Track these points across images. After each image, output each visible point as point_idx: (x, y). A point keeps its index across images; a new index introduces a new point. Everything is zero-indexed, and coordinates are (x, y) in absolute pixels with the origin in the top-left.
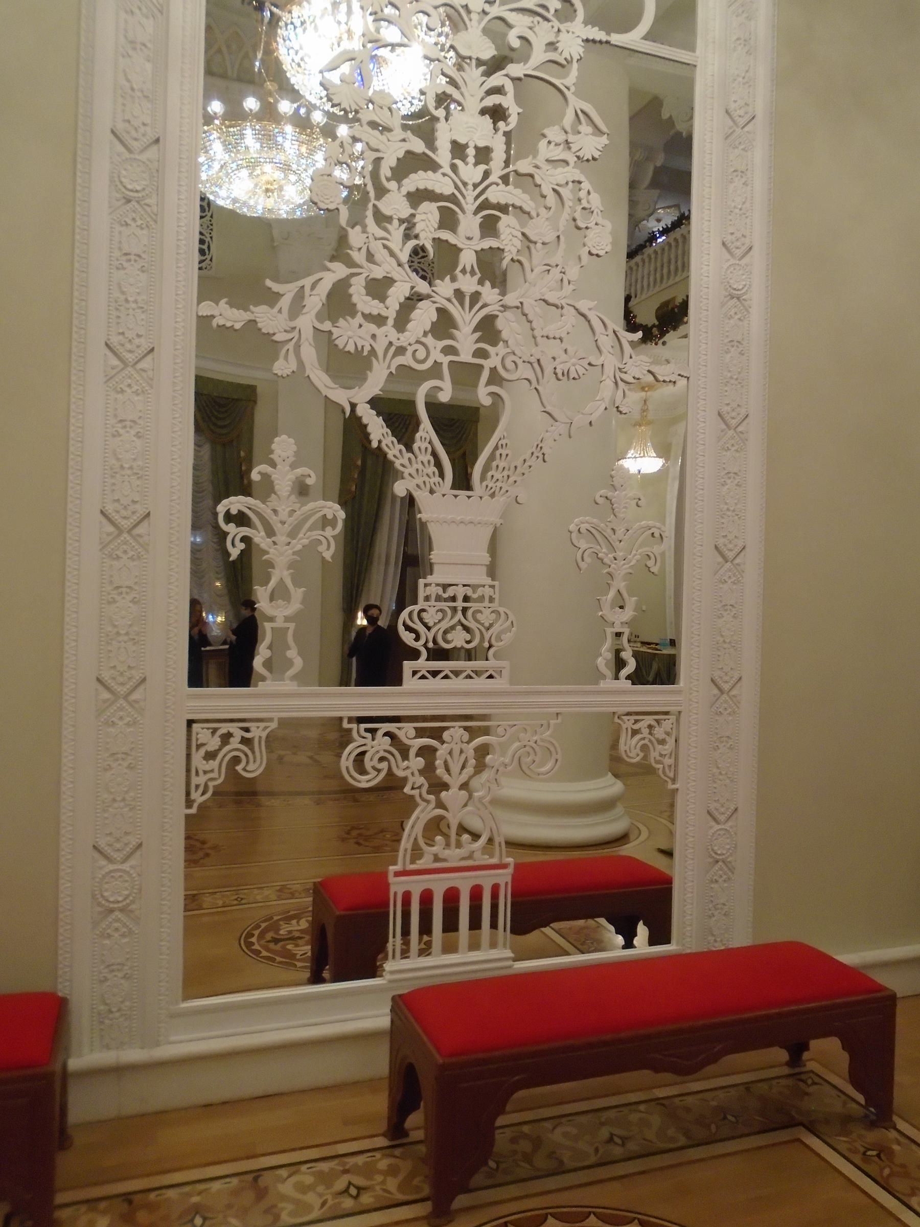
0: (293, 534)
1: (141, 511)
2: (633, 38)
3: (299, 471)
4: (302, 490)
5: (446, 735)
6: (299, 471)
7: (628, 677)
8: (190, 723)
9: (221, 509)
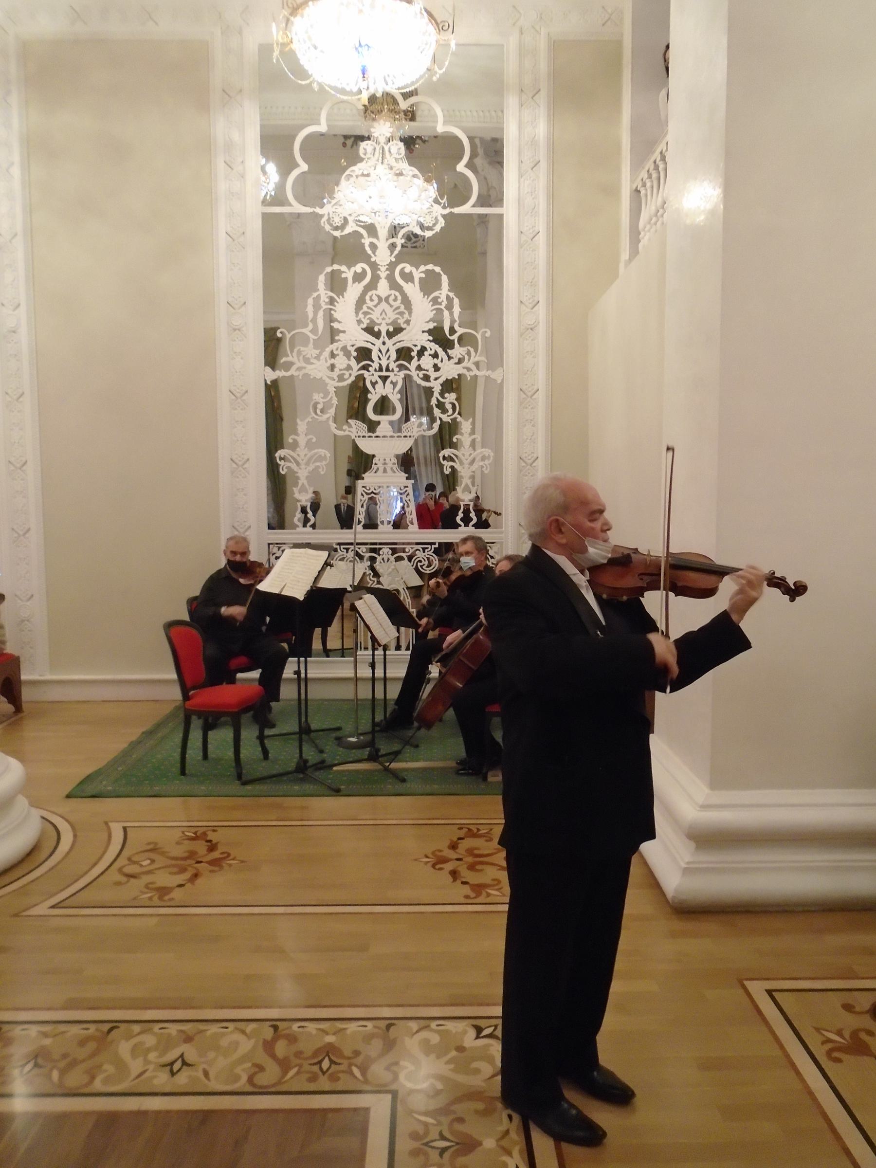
0: (307, 464)
1: (246, 457)
2: (466, 209)
3: (310, 437)
4: (309, 445)
6: (310, 437)
8: (269, 544)
9: (277, 455)
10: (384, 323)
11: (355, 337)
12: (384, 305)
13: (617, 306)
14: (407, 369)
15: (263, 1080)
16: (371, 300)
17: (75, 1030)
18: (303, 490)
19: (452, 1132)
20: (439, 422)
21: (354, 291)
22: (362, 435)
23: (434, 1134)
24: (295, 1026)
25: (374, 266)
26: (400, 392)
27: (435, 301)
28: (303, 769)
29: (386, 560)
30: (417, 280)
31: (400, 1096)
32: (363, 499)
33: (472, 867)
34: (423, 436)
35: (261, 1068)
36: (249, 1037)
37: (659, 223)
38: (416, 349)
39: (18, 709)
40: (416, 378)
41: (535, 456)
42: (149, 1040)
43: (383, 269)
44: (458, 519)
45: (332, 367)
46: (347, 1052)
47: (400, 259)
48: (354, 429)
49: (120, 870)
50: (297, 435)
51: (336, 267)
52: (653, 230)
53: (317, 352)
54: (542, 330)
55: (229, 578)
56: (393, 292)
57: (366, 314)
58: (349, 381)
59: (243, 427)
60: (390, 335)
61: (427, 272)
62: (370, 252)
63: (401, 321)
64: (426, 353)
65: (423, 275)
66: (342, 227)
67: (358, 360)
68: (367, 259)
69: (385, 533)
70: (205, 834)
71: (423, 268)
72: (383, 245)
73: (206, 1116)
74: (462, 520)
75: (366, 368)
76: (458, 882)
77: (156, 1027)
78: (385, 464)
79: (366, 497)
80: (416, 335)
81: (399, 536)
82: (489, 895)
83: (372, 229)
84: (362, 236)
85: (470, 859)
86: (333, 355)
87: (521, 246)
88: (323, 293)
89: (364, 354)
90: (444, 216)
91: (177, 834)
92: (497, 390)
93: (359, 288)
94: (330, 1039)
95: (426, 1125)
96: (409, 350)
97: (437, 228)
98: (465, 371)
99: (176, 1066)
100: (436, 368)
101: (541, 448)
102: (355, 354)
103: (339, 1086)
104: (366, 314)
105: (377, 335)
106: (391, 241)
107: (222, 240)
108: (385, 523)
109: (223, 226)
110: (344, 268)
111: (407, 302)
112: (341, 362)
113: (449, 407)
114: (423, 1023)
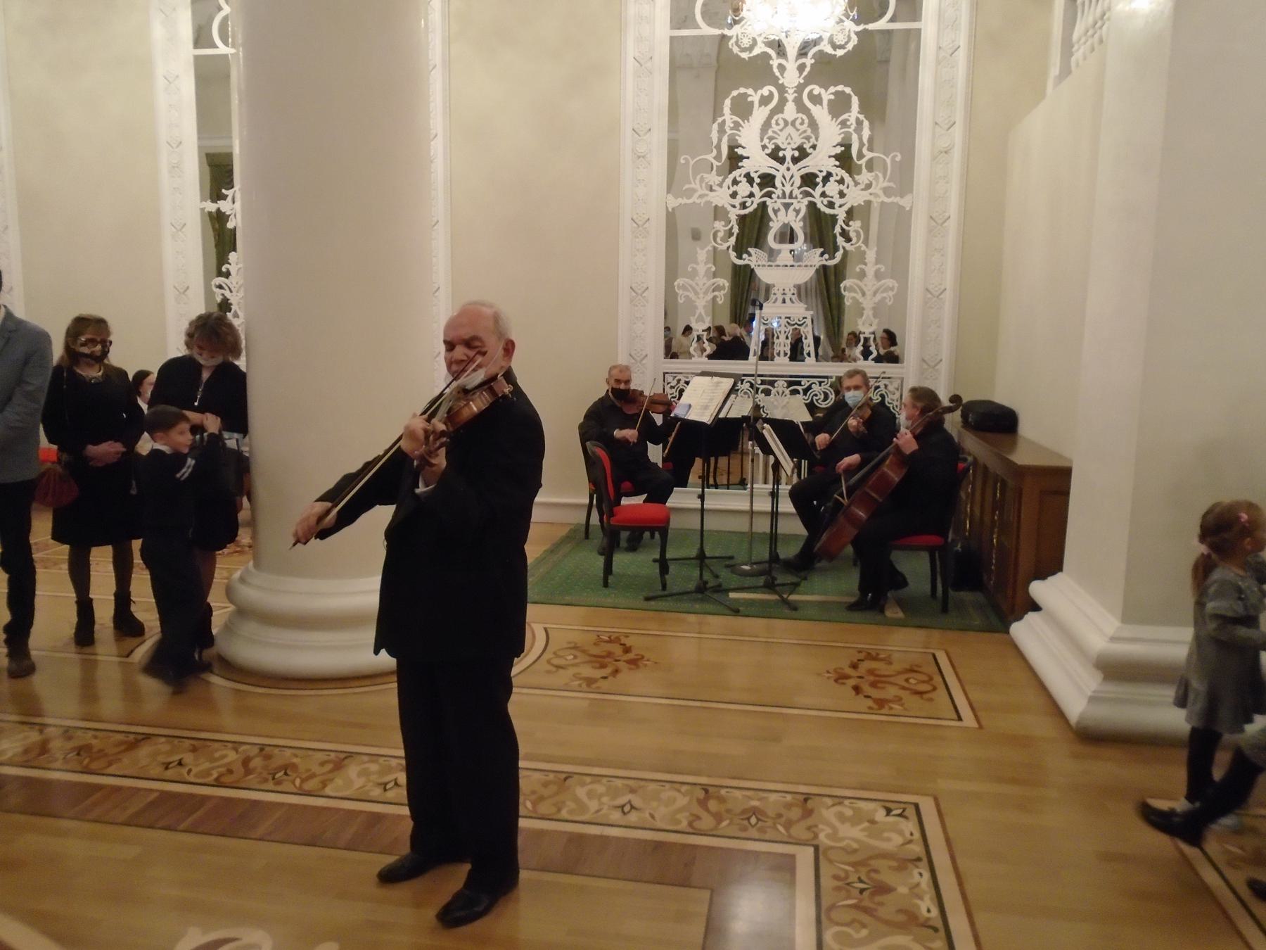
0: (706, 293)
2: (882, 24)
10: (789, 148)
11: (758, 162)
12: (790, 129)
13: (1045, 129)
14: (811, 195)
15: (698, 825)
16: (777, 124)
17: (537, 775)
18: (700, 319)
19: (870, 878)
20: (841, 251)
21: (760, 114)
23: (853, 878)
24: (723, 792)
25: (782, 89)
26: (804, 219)
27: (844, 124)
28: (702, 589)
30: (825, 102)
31: (821, 849)
33: (873, 685)
34: (824, 267)
35: (698, 818)
36: (684, 795)
37: (1097, 36)
38: (821, 175)
40: (820, 206)
42: (600, 789)
43: (791, 91)
45: (734, 195)
46: (771, 813)
47: (809, 80)
48: (754, 258)
49: (549, 662)
50: (697, 263)
51: (742, 90)
52: (1089, 43)
53: (720, 178)
54: (957, 154)
55: (613, 406)
56: (800, 115)
57: (771, 139)
58: (750, 209)
60: (795, 160)
61: (836, 94)
62: (778, 74)
63: (807, 146)
64: (832, 179)
65: (832, 97)
66: (751, 49)
67: (761, 186)
68: (774, 81)
70: (618, 639)
71: (832, 89)
72: (791, 65)
73: (658, 845)
75: (769, 195)
76: (861, 696)
77: (605, 780)
80: (821, 161)
82: (891, 708)
83: (779, 47)
84: (770, 57)
85: (872, 678)
86: (735, 182)
87: (938, 62)
88: (728, 117)
89: (767, 180)
90: (857, 33)
91: (593, 637)
92: (903, 218)
93: (766, 111)
94: (755, 803)
95: (846, 872)
96: (815, 176)
97: (850, 47)
98: (871, 198)
99: (627, 808)
100: (842, 195)
101: (949, 281)
102: (757, 180)
103: (767, 837)
104: (771, 139)
105: (782, 161)
106: (800, 61)
107: (630, 65)
109: (631, 50)
110: (750, 91)
111: (813, 125)
112: (744, 189)
113: (852, 235)
114: (837, 800)
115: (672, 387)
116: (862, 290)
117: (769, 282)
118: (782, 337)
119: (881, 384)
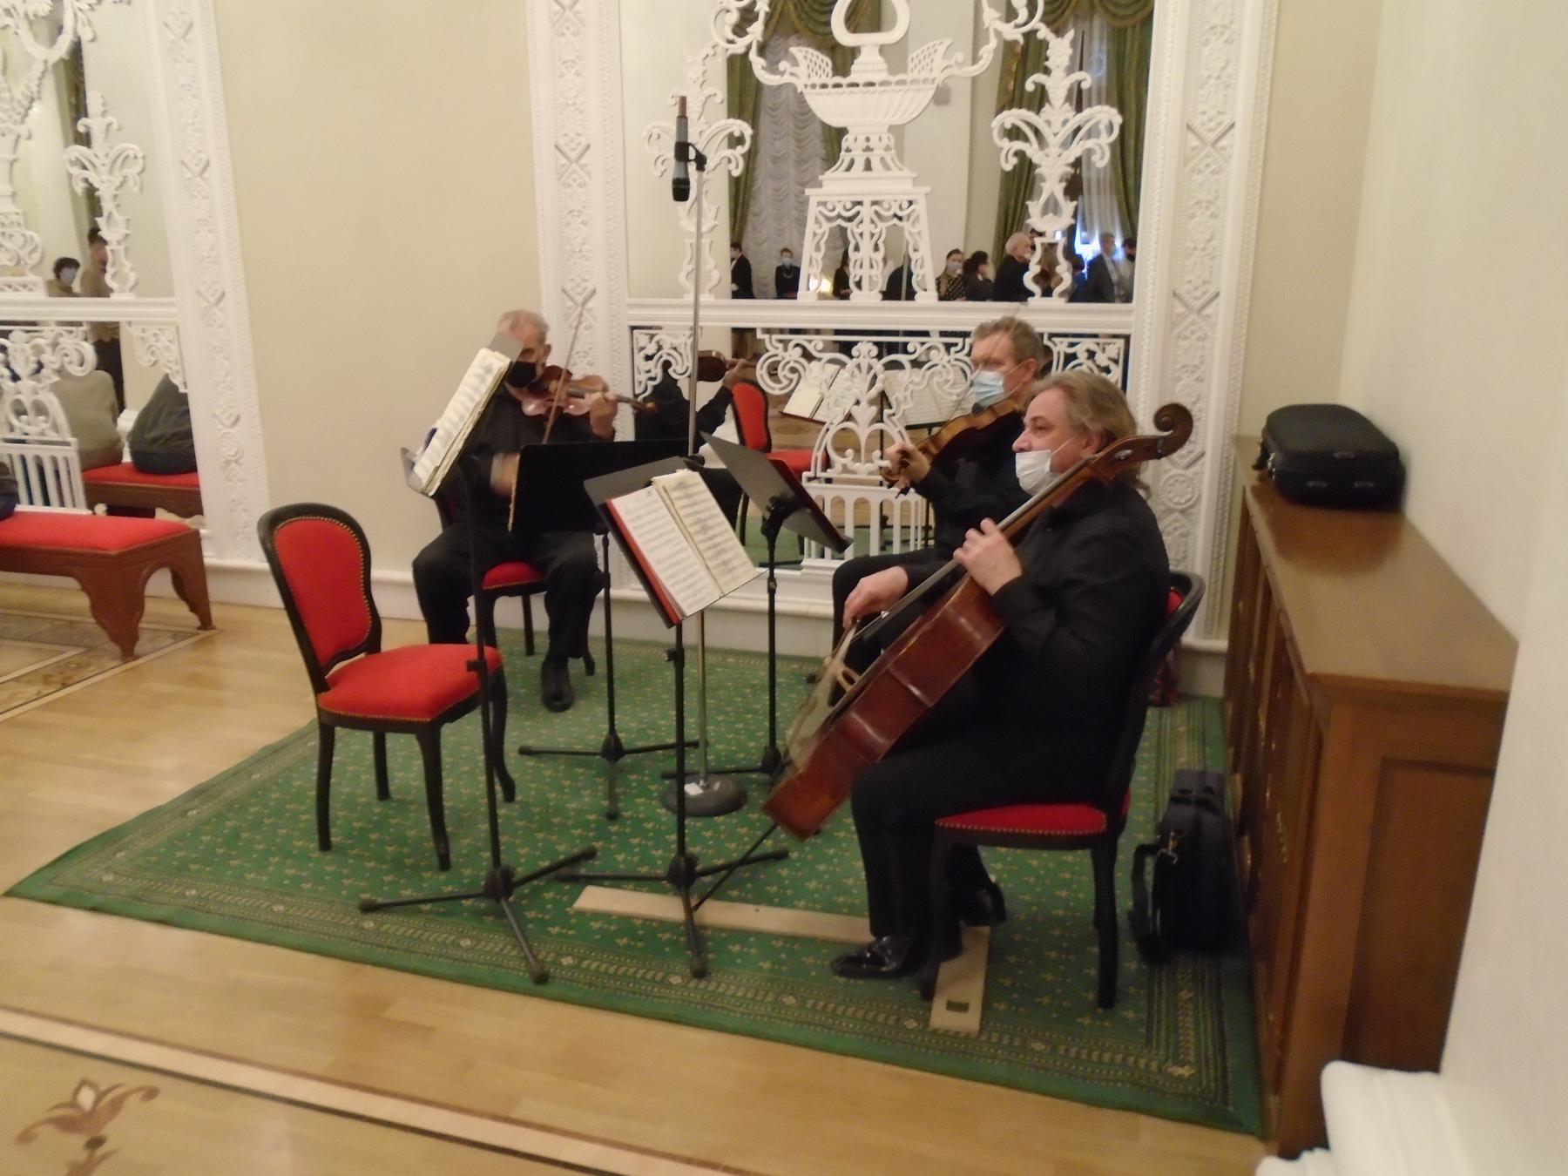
5: (854, 351)
7: (1061, 295)
20: (993, 43)
22: (818, 81)
29: (864, 368)
32: (820, 231)
39: (206, 623)
41: (1227, 121)
44: (1028, 280)
48: (802, 70)
59: (578, 74)
69: (867, 307)
74: (1037, 279)
78: (868, 149)
79: (826, 226)
81: (898, 316)
108: (865, 283)
115: (649, 358)
116: (1037, 132)
117: (835, 122)
118: (866, 245)
119: (1081, 350)
